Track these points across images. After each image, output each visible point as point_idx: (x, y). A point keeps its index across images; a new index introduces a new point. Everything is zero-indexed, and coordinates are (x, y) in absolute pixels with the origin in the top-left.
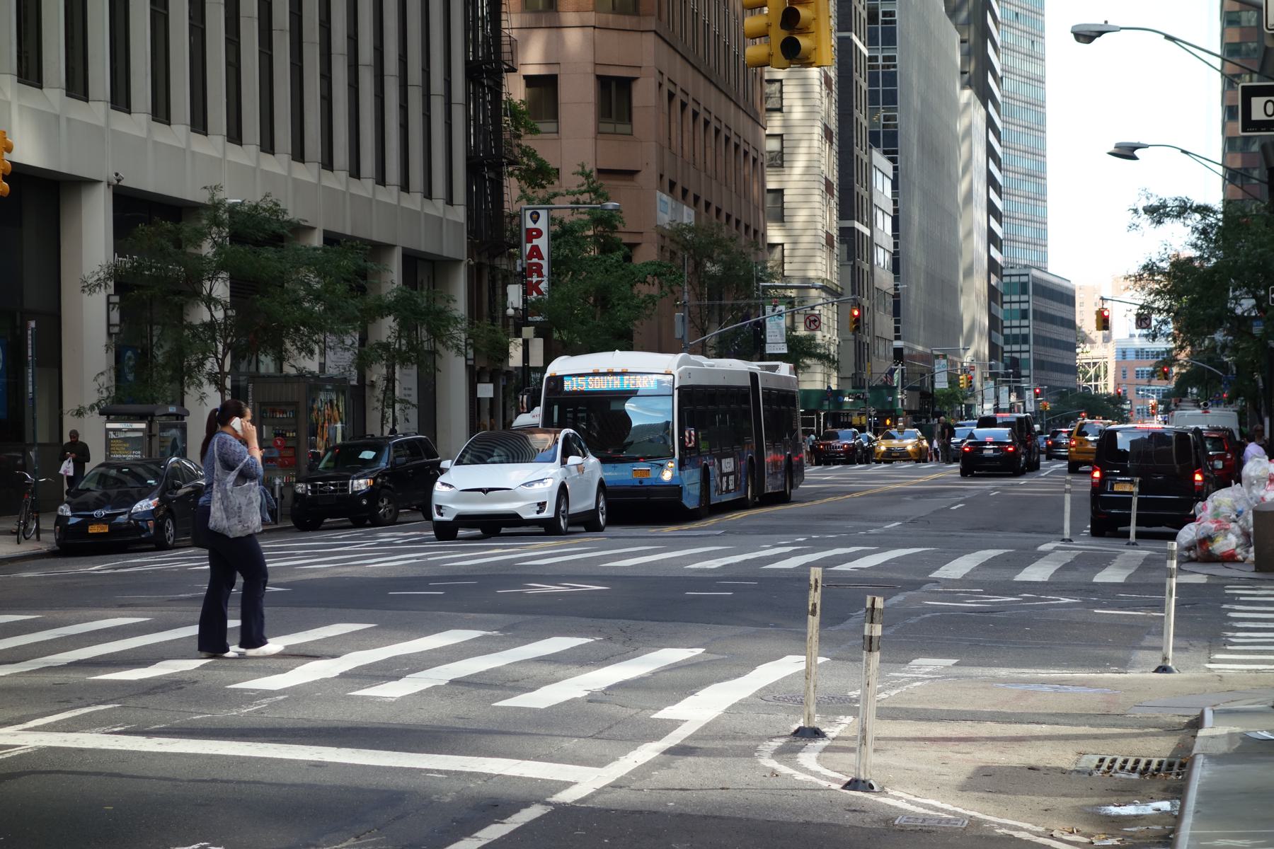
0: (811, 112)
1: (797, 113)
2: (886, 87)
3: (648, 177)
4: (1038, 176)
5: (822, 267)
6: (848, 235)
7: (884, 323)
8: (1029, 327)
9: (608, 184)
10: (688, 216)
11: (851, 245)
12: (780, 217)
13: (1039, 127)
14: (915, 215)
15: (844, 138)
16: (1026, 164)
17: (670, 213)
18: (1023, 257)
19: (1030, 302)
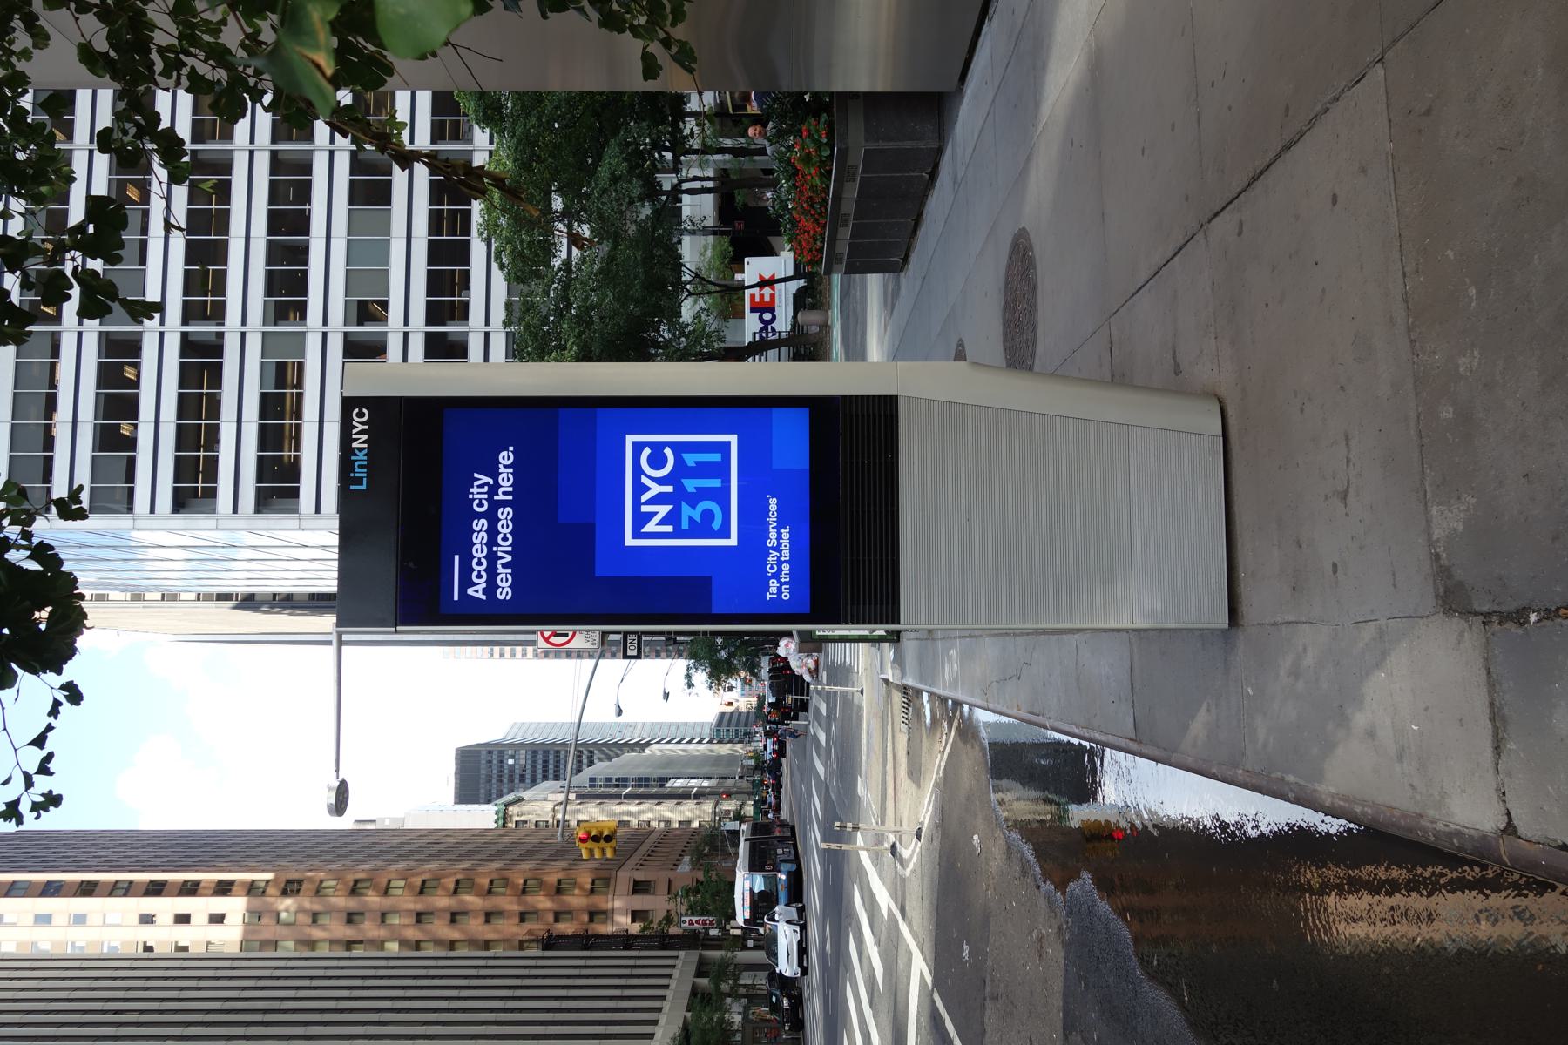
0: (651, 810)
1: (650, 815)
2: (643, 781)
3: (671, 874)
4: (678, 725)
5: (708, 806)
6: (697, 796)
7: (730, 782)
8: (733, 729)
9: (673, 891)
10: (687, 859)
11: (700, 795)
12: (689, 822)
13: (661, 725)
14: (691, 771)
15: (660, 798)
16: (673, 729)
17: (685, 867)
18: (707, 731)
19: (723, 729)
